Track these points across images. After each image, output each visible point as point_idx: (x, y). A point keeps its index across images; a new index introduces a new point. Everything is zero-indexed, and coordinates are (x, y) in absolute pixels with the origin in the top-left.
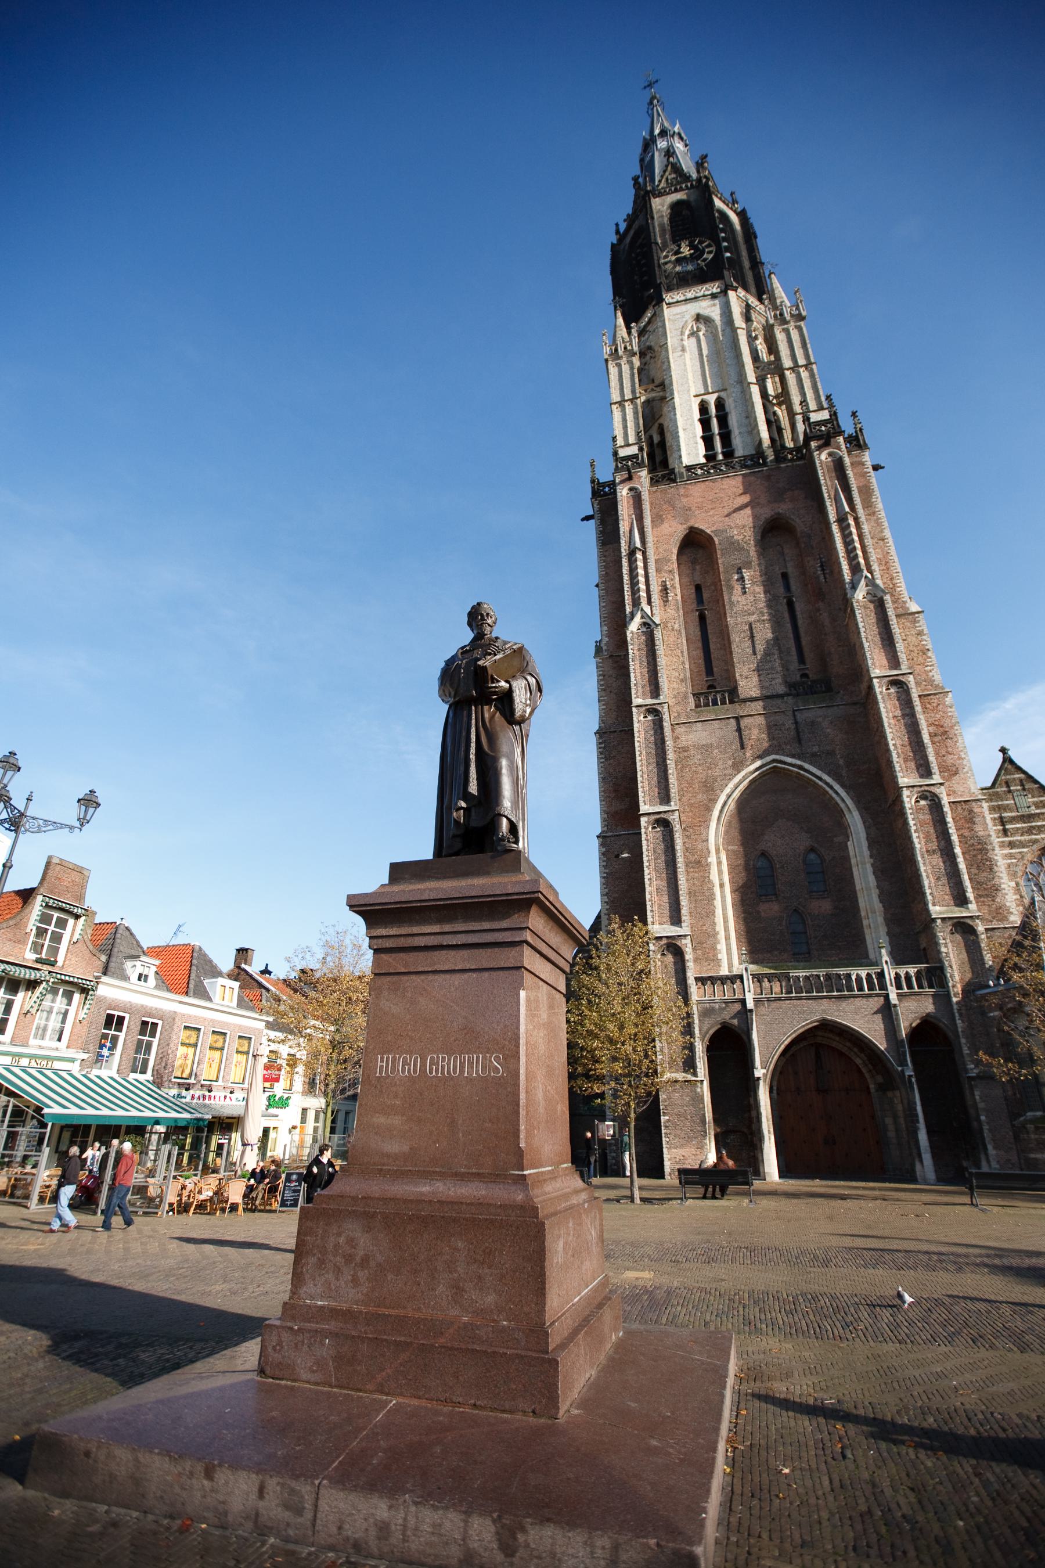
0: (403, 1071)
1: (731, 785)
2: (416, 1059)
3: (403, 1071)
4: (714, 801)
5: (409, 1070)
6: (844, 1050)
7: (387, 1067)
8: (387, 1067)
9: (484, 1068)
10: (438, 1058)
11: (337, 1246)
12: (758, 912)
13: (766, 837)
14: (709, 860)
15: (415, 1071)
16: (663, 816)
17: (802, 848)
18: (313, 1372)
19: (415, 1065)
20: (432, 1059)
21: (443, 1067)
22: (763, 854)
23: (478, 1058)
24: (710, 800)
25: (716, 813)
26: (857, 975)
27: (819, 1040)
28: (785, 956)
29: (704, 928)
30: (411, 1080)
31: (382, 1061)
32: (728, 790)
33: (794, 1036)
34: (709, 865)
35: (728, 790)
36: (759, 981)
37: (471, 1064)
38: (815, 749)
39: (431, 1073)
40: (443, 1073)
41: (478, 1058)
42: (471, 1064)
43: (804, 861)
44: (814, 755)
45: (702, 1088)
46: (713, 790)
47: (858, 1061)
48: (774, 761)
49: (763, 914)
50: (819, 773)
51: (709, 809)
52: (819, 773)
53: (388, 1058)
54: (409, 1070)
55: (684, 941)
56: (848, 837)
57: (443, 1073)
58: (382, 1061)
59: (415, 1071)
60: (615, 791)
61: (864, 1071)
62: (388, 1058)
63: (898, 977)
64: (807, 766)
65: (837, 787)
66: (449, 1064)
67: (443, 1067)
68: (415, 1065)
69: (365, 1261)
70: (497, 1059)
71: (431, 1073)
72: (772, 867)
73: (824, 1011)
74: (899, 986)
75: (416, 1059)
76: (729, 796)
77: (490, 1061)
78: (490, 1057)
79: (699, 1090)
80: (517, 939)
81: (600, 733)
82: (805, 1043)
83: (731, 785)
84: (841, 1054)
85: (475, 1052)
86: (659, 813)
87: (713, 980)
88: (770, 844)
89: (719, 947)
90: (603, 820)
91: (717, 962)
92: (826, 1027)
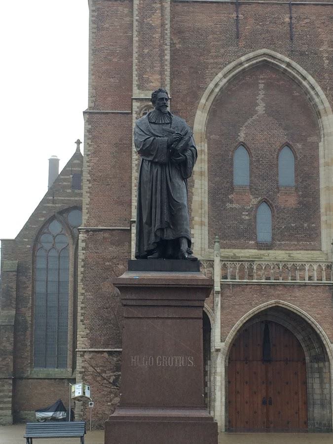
6: (290, 328)
9: (185, 362)
10: (162, 358)
15: (151, 364)
25: (203, 101)
27: (269, 319)
37: (178, 361)
38: (305, 48)
39: (159, 364)
42: (178, 361)
44: (302, 54)
47: (300, 337)
48: (265, 54)
50: (304, 72)
52: (304, 72)
56: (320, 138)
58: (134, 359)
59: (151, 364)
61: (303, 345)
64: (294, 64)
65: (318, 88)
66: (168, 361)
70: (191, 359)
71: (159, 364)
82: (257, 320)
84: (286, 330)
90: (91, 96)
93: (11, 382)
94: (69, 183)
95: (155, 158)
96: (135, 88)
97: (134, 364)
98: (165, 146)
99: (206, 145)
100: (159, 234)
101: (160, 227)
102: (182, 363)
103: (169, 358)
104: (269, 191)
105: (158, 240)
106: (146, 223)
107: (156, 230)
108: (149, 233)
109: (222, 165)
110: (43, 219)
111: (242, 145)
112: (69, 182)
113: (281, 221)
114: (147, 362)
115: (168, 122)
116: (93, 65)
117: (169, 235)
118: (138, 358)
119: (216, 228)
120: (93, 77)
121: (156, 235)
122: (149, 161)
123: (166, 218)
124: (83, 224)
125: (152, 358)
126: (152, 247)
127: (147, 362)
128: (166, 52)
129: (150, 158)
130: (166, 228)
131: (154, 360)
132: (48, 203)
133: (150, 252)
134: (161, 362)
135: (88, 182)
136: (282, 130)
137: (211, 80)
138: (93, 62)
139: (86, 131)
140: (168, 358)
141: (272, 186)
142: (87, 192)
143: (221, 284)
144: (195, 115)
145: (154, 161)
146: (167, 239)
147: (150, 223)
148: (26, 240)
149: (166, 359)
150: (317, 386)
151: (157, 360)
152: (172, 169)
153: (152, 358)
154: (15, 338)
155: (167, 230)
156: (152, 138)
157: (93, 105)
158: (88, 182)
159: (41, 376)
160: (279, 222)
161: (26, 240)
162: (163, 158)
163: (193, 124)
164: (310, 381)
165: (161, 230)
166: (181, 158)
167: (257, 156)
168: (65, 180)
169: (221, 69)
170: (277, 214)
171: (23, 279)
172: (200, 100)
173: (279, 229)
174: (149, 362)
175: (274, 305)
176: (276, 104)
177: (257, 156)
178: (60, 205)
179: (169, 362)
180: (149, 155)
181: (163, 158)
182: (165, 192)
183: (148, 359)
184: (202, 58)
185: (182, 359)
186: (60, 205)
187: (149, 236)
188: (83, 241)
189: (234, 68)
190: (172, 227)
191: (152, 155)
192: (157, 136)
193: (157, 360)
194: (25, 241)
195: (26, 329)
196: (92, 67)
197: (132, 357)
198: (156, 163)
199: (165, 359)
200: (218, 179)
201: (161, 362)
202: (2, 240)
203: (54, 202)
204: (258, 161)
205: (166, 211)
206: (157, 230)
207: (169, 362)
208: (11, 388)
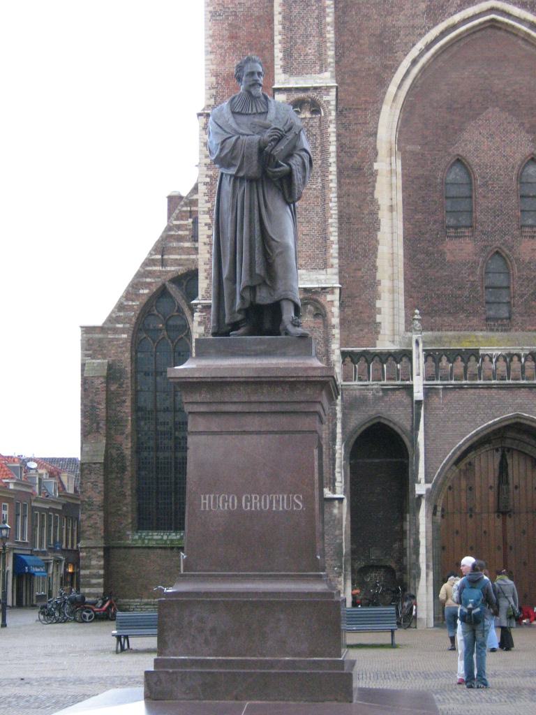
0: (224, 506)
1: (420, 45)
3: (224, 506)
4: (393, 69)
5: (228, 506)
10: (251, 497)
11: (190, 623)
12: (442, 254)
13: (466, 136)
14: (376, 166)
16: (310, 94)
17: (518, 157)
18: (187, 694)
20: (247, 498)
21: (256, 504)
22: (459, 161)
23: (283, 498)
24: (386, 67)
25: (392, 89)
28: (475, 321)
29: (360, 274)
30: (230, 513)
31: (205, 499)
32: (414, 52)
33: (475, 439)
34: (374, 174)
35: (414, 52)
36: (434, 361)
37: (278, 502)
39: (246, 506)
40: (256, 508)
41: (283, 498)
42: (278, 502)
43: (520, 176)
45: (340, 508)
46: (391, 50)
49: (448, 257)
51: (383, 83)
53: (210, 497)
55: (329, 297)
57: (256, 508)
58: (205, 499)
60: (233, 37)
62: (210, 497)
66: (260, 501)
67: (256, 504)
69: (213, 631)
71: (246, 506)
72: (471, 183)
73: (520, 406)
76: (414, 62)
77: (293, 501)
78: (293, 497)
79: (336, 511)
80: (312, 410)
81: (379, 229)
83: (420, 45)
85: (280, 493)
86: (305, 89)
87: (368, 357)
88: (470, 147)
89: (378, 304)
91: (374, 328)
93: (101, 553)
94: (187, 233)
95: (238, 171)
96: (278, 70)
97: (205, 507)
98: (255, 150)
99: (399, 163)
100: (247, 295)
101: (249, 284)
104: (505, 234)
105: (247, 305)
106: (227, 279)
108: (233, 293)
109: (426, 194)
110: (146, 291)
111: (458, 160)
112: (187, 230)
113: (525, 283)
114: (226, 504)
115: (263, 111)
116: (211, 36)
117: (263, 297)
119: (418, 298)
120: (212, 57)
121: (242, 298)
122: (231, 176)
123: (259, 270)
124: (200, 297)
126: (239, 317)
127: (226, 504)
128: (328, 10)
129: (233, 171)
130: (259, 285)
131: (238, 500)
132: (155, 265)
133: (235, 326)
134: (249, 504)
135: (207, 227)
136: (523, 133)
137: (406, 55)
138: (211, 32)
139: (202, 144)
140: (260, 499)
141: (509, 225)
142: (205, 244)
143: (424, 388)
144: (379, 113)
146: (261, 302)
147: (233, 278)
148: (120, 326)
149: (258, 499)
151: (244, 501)
152: (267, 192)
154: (106, 482)
156: (234, 139)
157: (212, 102)
158: (207, 227)
159: (153, 544)
160: (521, 285)
161: (120, 326)
163: (377, 128)
165: (252, 289)
166: (282, 168)
167: (484, 178)
168: (179, 227)
169: (421, 35)
170: (519, 272)
172: (388, 87)
173: (521, 297)
174: (230, 504)
175: (513, 421)
176: (514, 90)
177: (484, 178)
178: (173, 268)
179: (263, 503)
180: (229, 166)
181: (253, 169)
182: (257, 227)
184: (389, 19)
185: (283, 499)
186: (173, 268)
188: (200, 323)
189: (443, 34)
190: (268, 283)
191: (235, 165)
192: (243, 135)
193: (244, 501)
194: (118, 328)
195: (123, 469)
196: (210, 40)
197: (202, 496)
198: (242, 179)
199: (256, 498)
200: (419, 216)
201: (249, 504)
202: (81, 327)
203: (163, 263)
204: (485, 184)
205: (258, 257)
206: (244, 289)
207: (263, 503)
208: (102, 563)
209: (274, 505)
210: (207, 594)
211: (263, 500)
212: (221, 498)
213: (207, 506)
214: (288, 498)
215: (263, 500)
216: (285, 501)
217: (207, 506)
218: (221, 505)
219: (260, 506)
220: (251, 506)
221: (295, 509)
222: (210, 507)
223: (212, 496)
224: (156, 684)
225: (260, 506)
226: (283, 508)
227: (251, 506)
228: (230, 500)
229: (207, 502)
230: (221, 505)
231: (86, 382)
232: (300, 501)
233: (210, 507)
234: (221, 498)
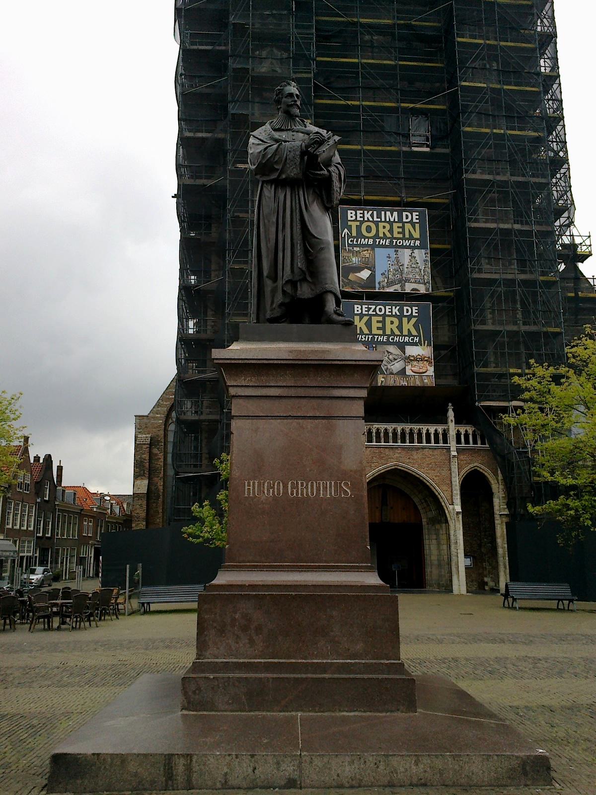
2: (279, 483)
5: (273, 492)
6: (407, 491)
7: (254, 488)
8: (254, 488)
10: (297, 483)
11: (234, 620)
15: (279, 493)
18: (230, 704)
19: (278, 489)
21: (302, 492)
23: (331, 483)
26: (428, 430)
37: (325, 488)
39: (292, 494)
40: (302, 494)
41: (331, 483)
42: (325, 488)
47: (416, 500)
53: (254, 483)
54: (273, 492)
57: (302, 494)
59: (279, 493)
61: (419, 507)
62: (254, 483)
63: (458, 435)
66: (307, 488)
67: (302, 492)
68: (278, 489)
69: (259, 629)
70: (346, 484)
71: (292, 494)
74: (459, 441)
75: (279, 483)
78: (340, 483)
92: (397, 473)
98: (298, 153)
100: (288, 289)
102: (331, 493)
103: (310, 484)
107: (284, 282)
114: (271, 491)
117: (305, 291)
118: (256, 484)
121: (284, 292)
123: (300, 263)
125: (281, 485)
126: (277, 313)
127: (271, 491)
130: (300, 280)
145: (280, 178)
148: (159, 416)
150: (434, 548)
151: (289, 487)
153: (281, 485)
154: (148, 505)
155: (301, 285)
156: (275, 146)
162: (293, 171)
164: (426, 542)
165: (293, 283)
166: (322, 172)
171: (155, 451)
174: (276, 490)
179: (309, 490)
181: (293, 171)
183: (274, 485)
187: (273, 297)
190: (309, 279)
193: (289, 487)
195: (158, 497)
199: (302, 485)
205: (299, 252)
206: (287, 282)
207: (309, 490)
209: (321, 492)
210: (253, 587)
211: (309, 486)
212: (266, 484)
213: (251, 491)
214: (336, 484)
215: (309, 486)
216: (333, 488)
217: (251, 491)
218: (266, 492)
219: (307, 494)
220: (297, 492)
221: (343, 496)
222: (254, 492)
223: (256, 482)
224: (194, 692)
225: (307, 494)
226: (331, 493)
227: (297, 492)
228: (276, 487)
229: (251, 488)
230: (266, 492)
231: (137, 447)
232: (349, 488)
233: (254, 492)
234: (266, 484)
